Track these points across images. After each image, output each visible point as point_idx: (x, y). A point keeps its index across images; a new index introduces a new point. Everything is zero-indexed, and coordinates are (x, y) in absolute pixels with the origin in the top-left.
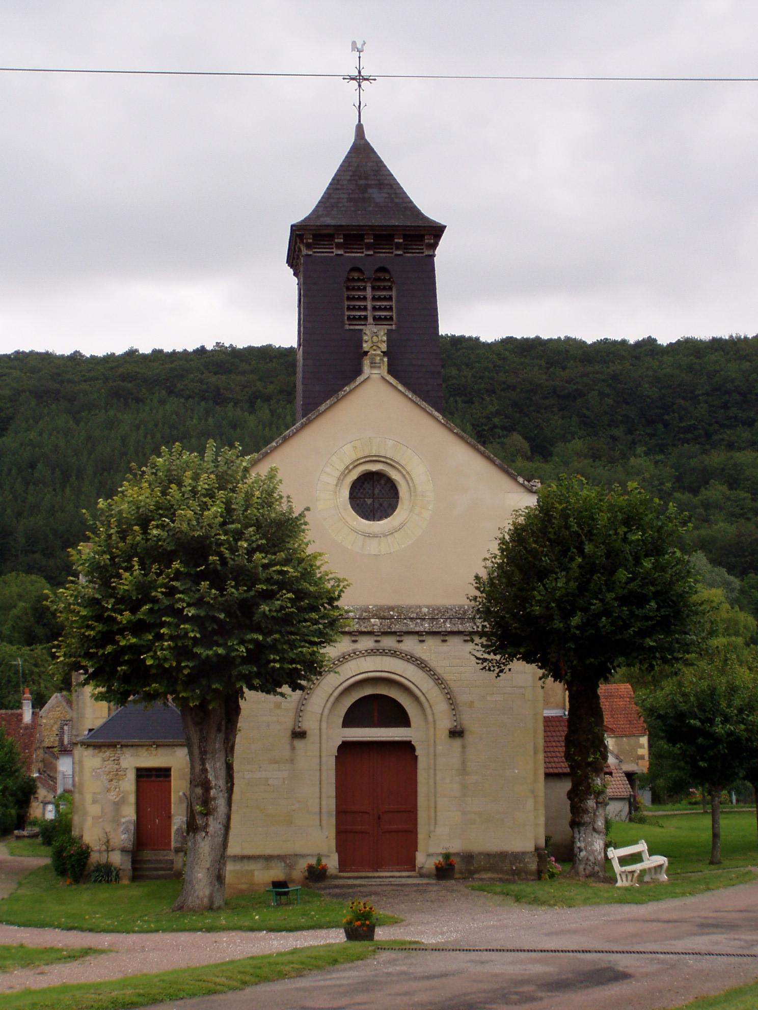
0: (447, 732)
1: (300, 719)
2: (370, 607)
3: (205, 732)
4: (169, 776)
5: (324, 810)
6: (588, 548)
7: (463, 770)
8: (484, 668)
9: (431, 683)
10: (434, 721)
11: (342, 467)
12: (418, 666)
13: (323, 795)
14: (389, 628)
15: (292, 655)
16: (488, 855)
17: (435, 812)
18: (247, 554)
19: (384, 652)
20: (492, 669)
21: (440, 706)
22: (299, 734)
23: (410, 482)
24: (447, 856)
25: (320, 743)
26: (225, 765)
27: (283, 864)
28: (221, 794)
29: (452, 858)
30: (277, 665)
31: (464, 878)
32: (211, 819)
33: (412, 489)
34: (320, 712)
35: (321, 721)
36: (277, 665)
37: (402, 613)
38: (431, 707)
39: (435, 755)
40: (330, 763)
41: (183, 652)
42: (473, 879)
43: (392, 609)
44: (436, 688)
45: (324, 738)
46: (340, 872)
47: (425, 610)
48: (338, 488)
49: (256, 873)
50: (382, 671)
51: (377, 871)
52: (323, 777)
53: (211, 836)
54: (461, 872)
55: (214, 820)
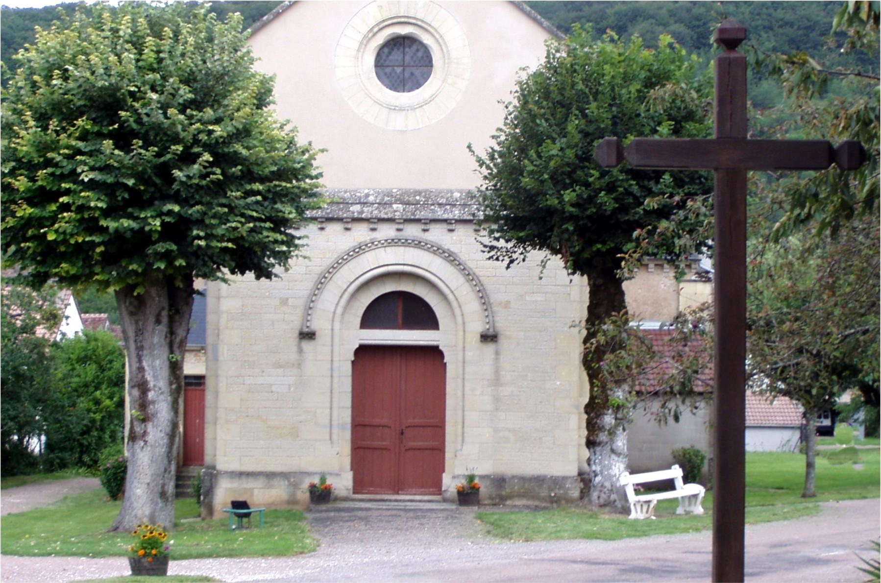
0: (478, 336)
1: (309, 318)
2: (394, 191)
3: (140, 323)
4: (203, 384)
5: (335, 423)
6: (592, 108)
7: (497, 381)
8: (492, 257)
9: (462, 279)
10: (464, 323)
11: (365, 30)
12: (446, 259)
13: (335, 405)
14: (413, 214)
15: (220, 231)
16: (523, 479)
17: (463, 427)
18: (160, 108)
19: (406, 243)
20: (501, 258)
21: (471, 305)
22: (307, 335)
23: (444, 47)
24: (471, 478)
25: (332, 345)
26: (167, 363)
27: (286, 483)
28: (162, 397)
29: (476, 481)
30: (202, 243)
31: (494, 505)
32: (150, 426)
33: (446, 55)
34: (332, 310)
35: (333, 321)
36: (202, 243)
37: (429, 198)
38: (460, 307)
39: (464, 362)
40: (347, 369)
41: (90, 225)
42: (504, 505)
43: (419, 193)
44: (467, 285)
45: (336, 340)
46: (354, 493)
47: (457, 195)
48: (360, 54)
49: (256, 492)
50: (404, 265)
51: (398, 494)
52: (335, 385)
53: (151, 446)
54: (491, 498)
55: (153, 427)
